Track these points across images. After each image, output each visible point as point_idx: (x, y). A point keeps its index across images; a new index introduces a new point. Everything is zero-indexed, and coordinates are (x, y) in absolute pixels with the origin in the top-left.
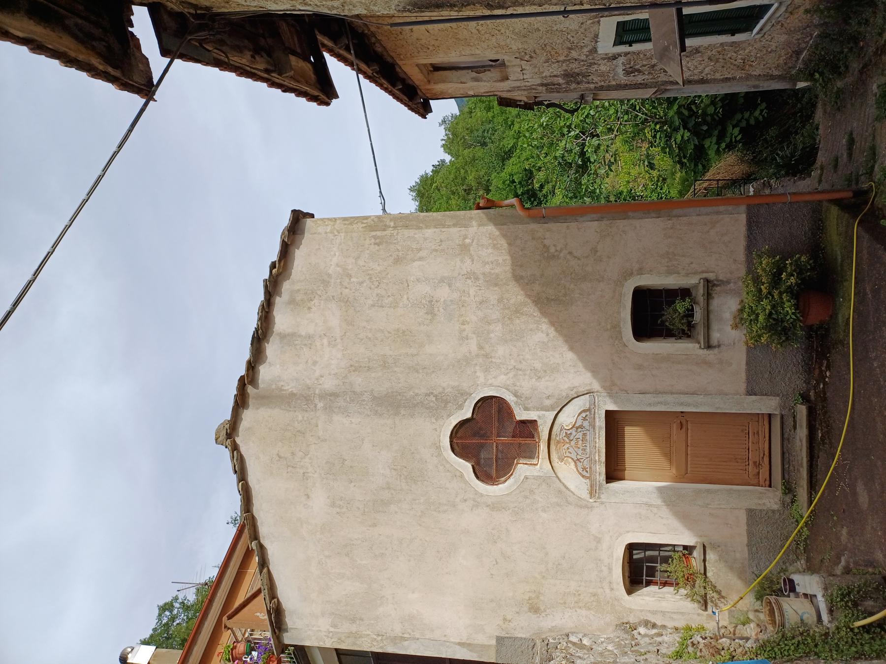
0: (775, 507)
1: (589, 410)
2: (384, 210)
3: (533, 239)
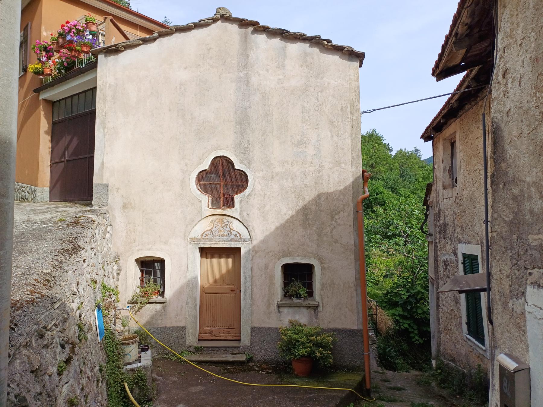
0: (187, 342)
1: (241, 238)
2: (364, 112)
3: (344, 206)
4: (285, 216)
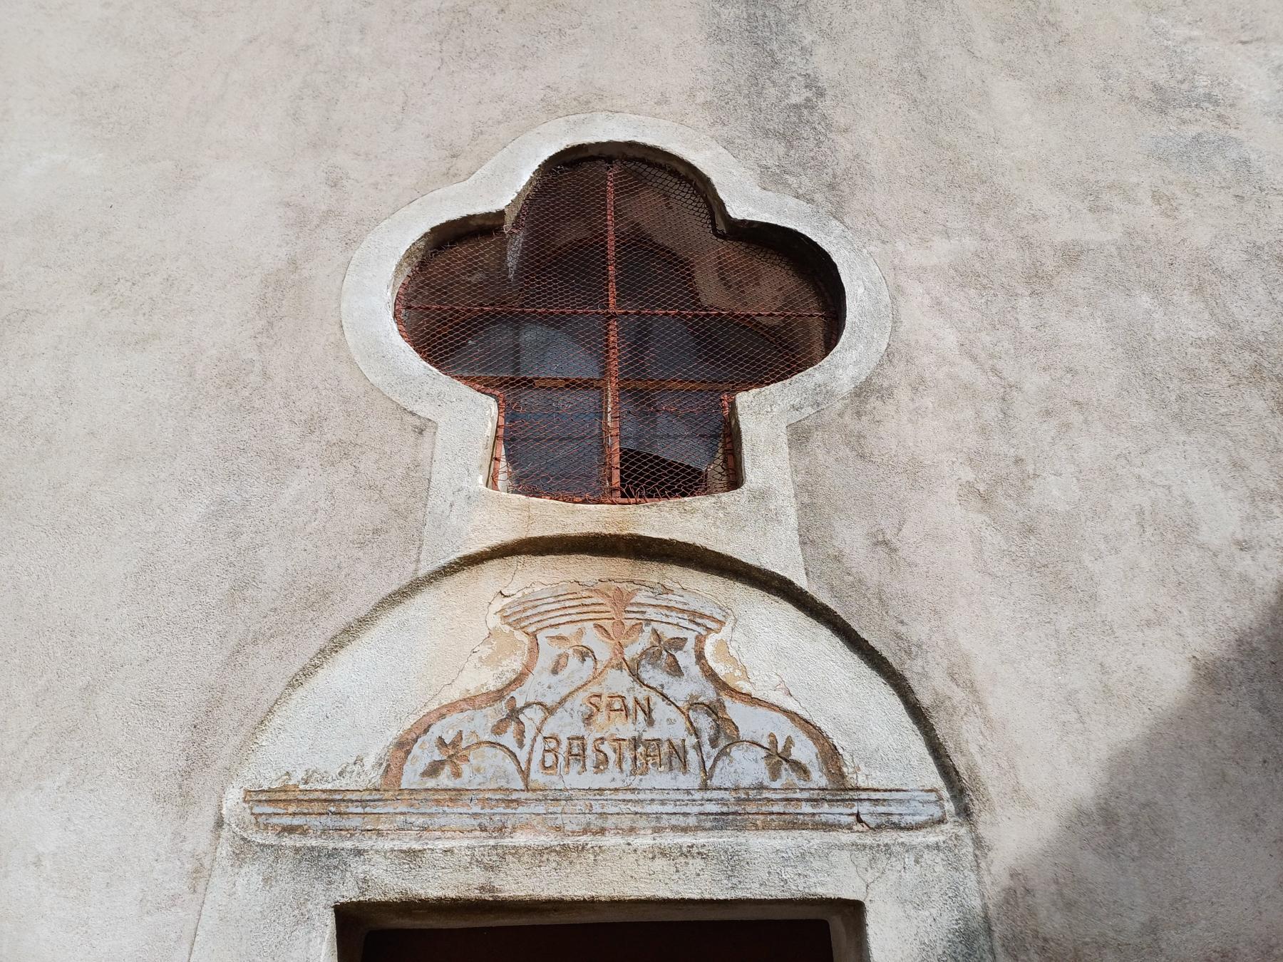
1: (841, 789)
4: (1245, 564)
